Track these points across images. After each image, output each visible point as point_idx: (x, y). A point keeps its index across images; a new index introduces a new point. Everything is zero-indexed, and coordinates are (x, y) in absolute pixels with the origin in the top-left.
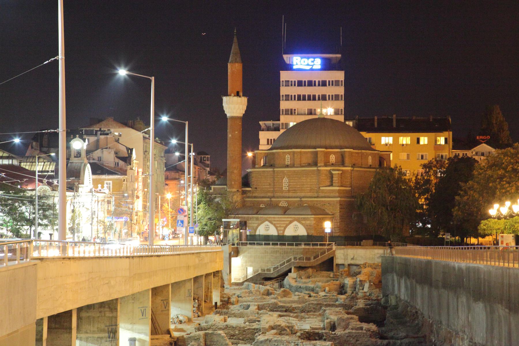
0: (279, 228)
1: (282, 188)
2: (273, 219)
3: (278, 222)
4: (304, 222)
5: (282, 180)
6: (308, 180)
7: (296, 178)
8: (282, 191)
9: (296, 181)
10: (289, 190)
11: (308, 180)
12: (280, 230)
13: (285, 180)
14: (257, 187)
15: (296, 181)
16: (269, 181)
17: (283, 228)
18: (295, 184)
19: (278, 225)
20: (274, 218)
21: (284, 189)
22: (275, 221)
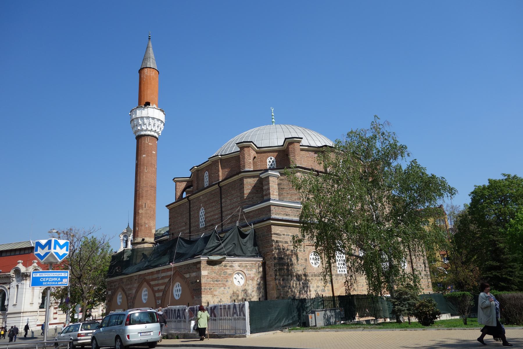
0: (157, 295)
1: (198, 225)
2: (150, 277)
3: (156, 282)
4: (187, 276)
5: (198, 212)
6: (228, 202)
7: (214, 204)
8: (199, 231)
9: (214, 209)
10: (205, 227)
11: (228, 202)
12: (158, 298)
13: (202, 212)
14: (173, 232)
15: (214, 209)
16: (184, 220)
17: (161, 294)
18: (212, 213)
19: (156, 288)
20: (152, 273)
21: (201, 227)
22: (153, 280)
